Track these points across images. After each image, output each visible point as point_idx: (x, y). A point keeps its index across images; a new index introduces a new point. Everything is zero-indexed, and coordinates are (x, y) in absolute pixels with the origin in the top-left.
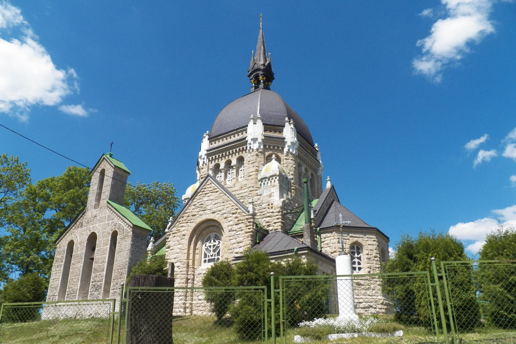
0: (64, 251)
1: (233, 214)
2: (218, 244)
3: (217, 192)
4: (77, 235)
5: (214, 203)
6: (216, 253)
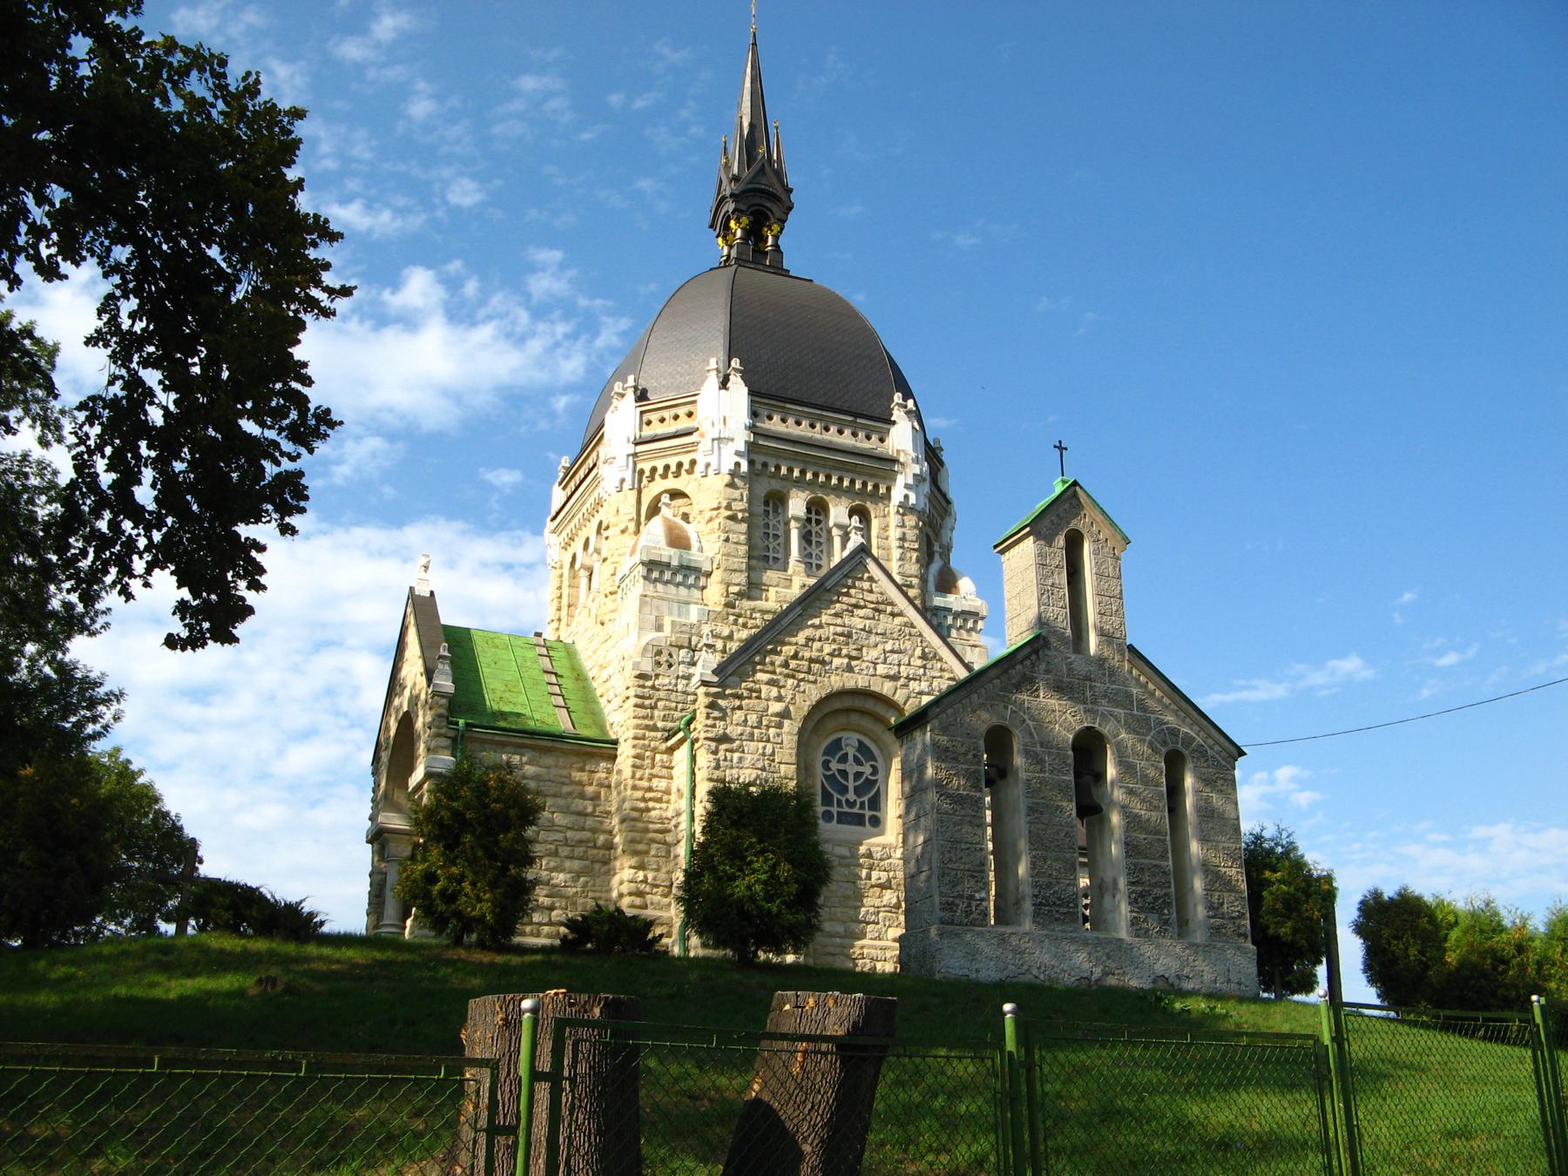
2: (872, 774)
3: (893, 615)
5: (888, 647)
6: (866, 799)
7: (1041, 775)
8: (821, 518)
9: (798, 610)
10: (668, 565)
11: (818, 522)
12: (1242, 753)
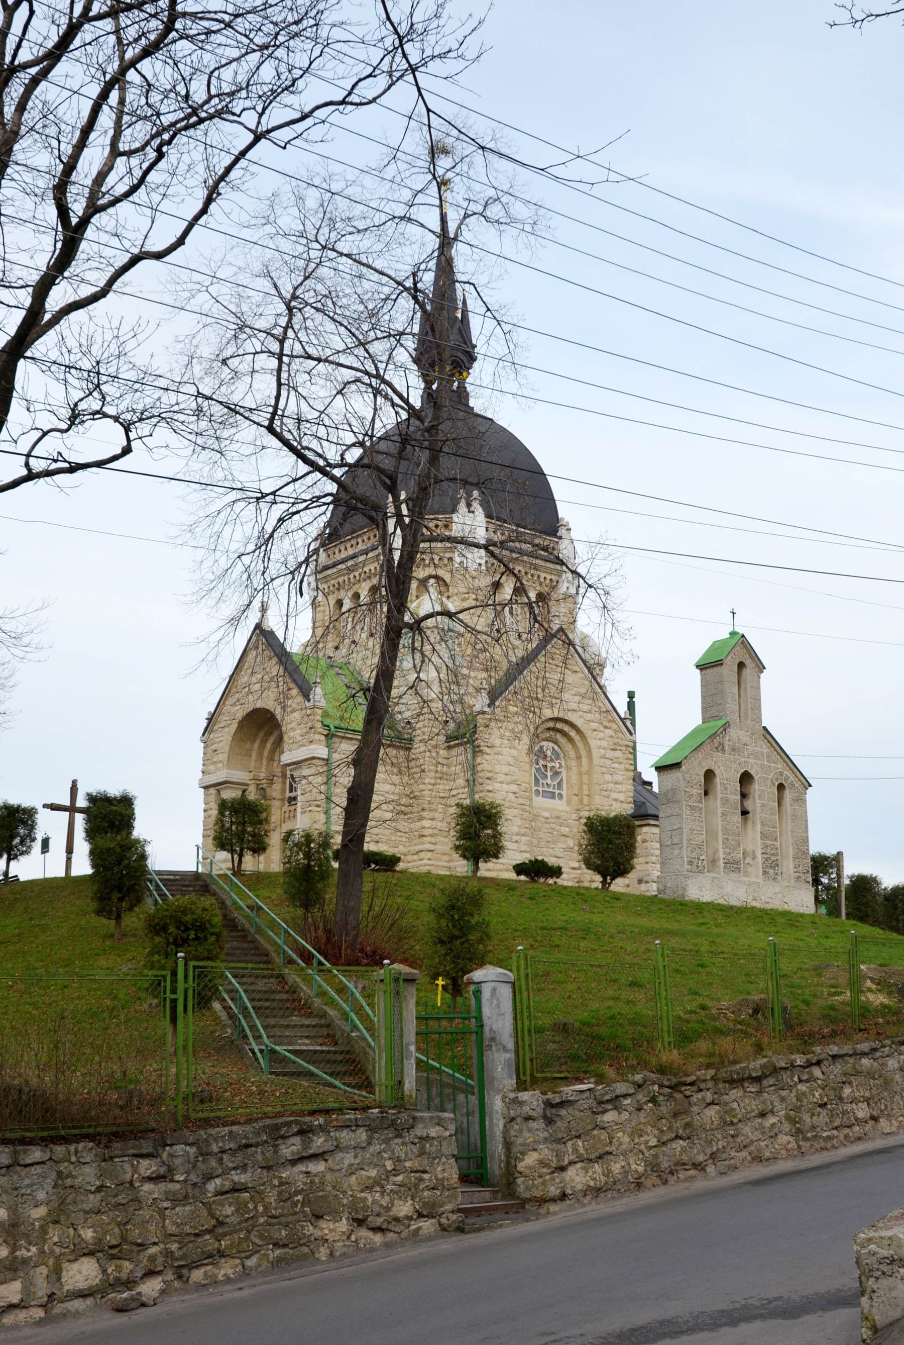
1: (606, 727)
6: (556, 783)
12: (810, 786)
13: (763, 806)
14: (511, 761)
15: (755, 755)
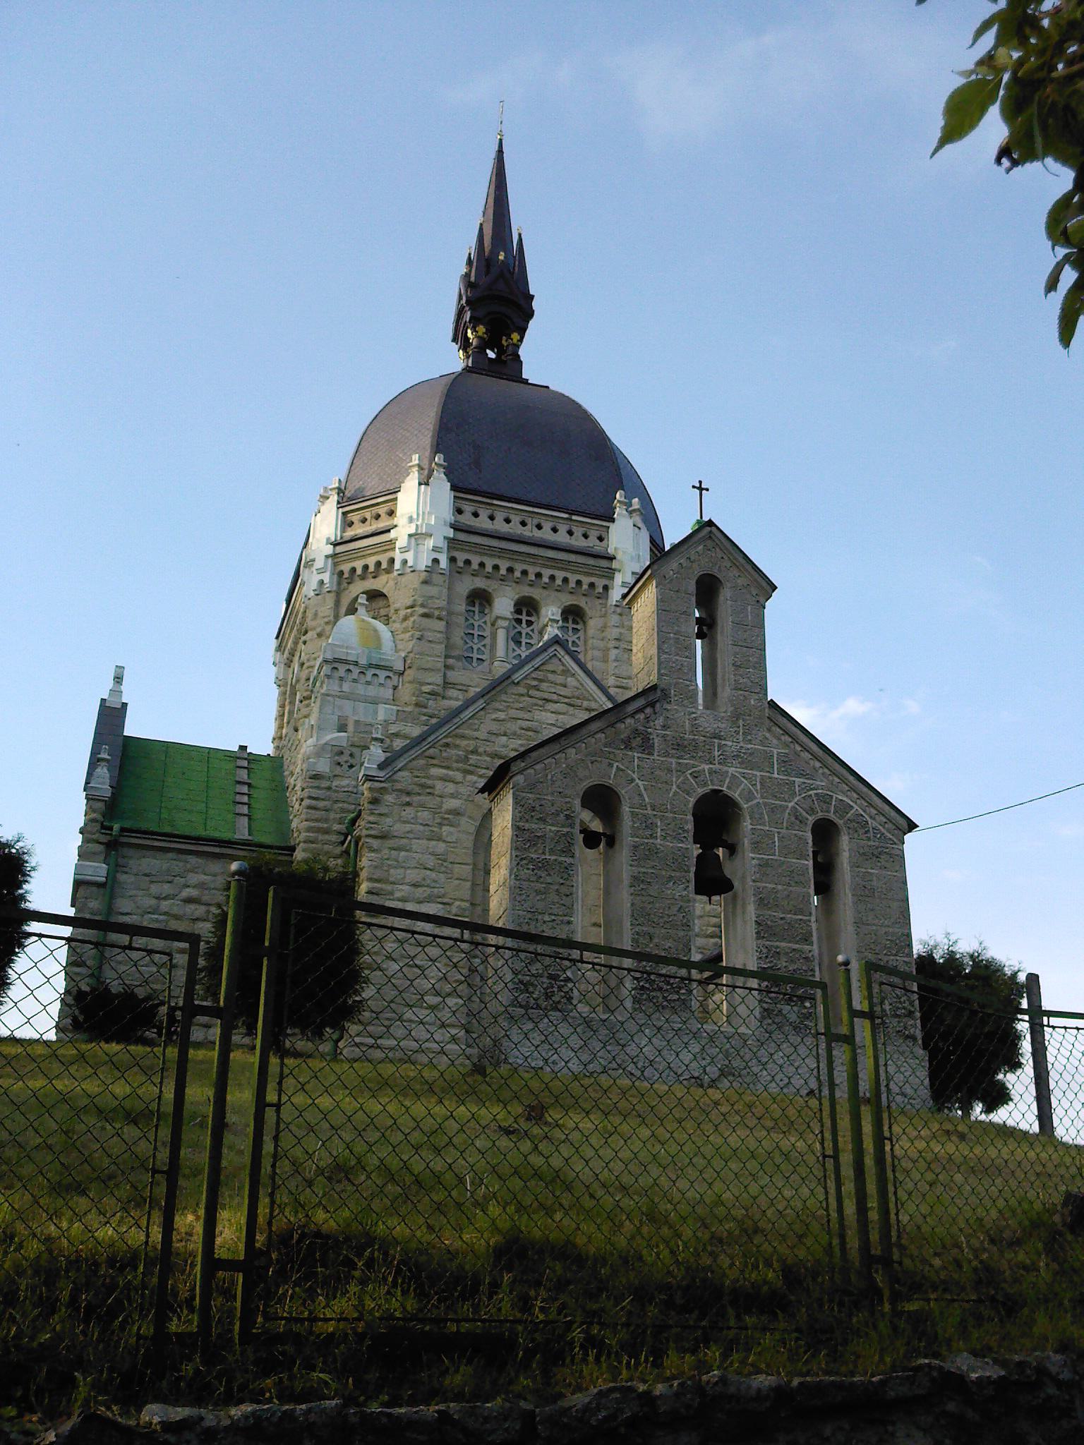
0: (568, 817)
4: (635, 776)
7: (651, 841)
8: (532, 619)
9: (480, 703)
10: (356, 663)
11: (529, 623)
13: (764, 865)
14: (431, 862)
15: (746, 760)
